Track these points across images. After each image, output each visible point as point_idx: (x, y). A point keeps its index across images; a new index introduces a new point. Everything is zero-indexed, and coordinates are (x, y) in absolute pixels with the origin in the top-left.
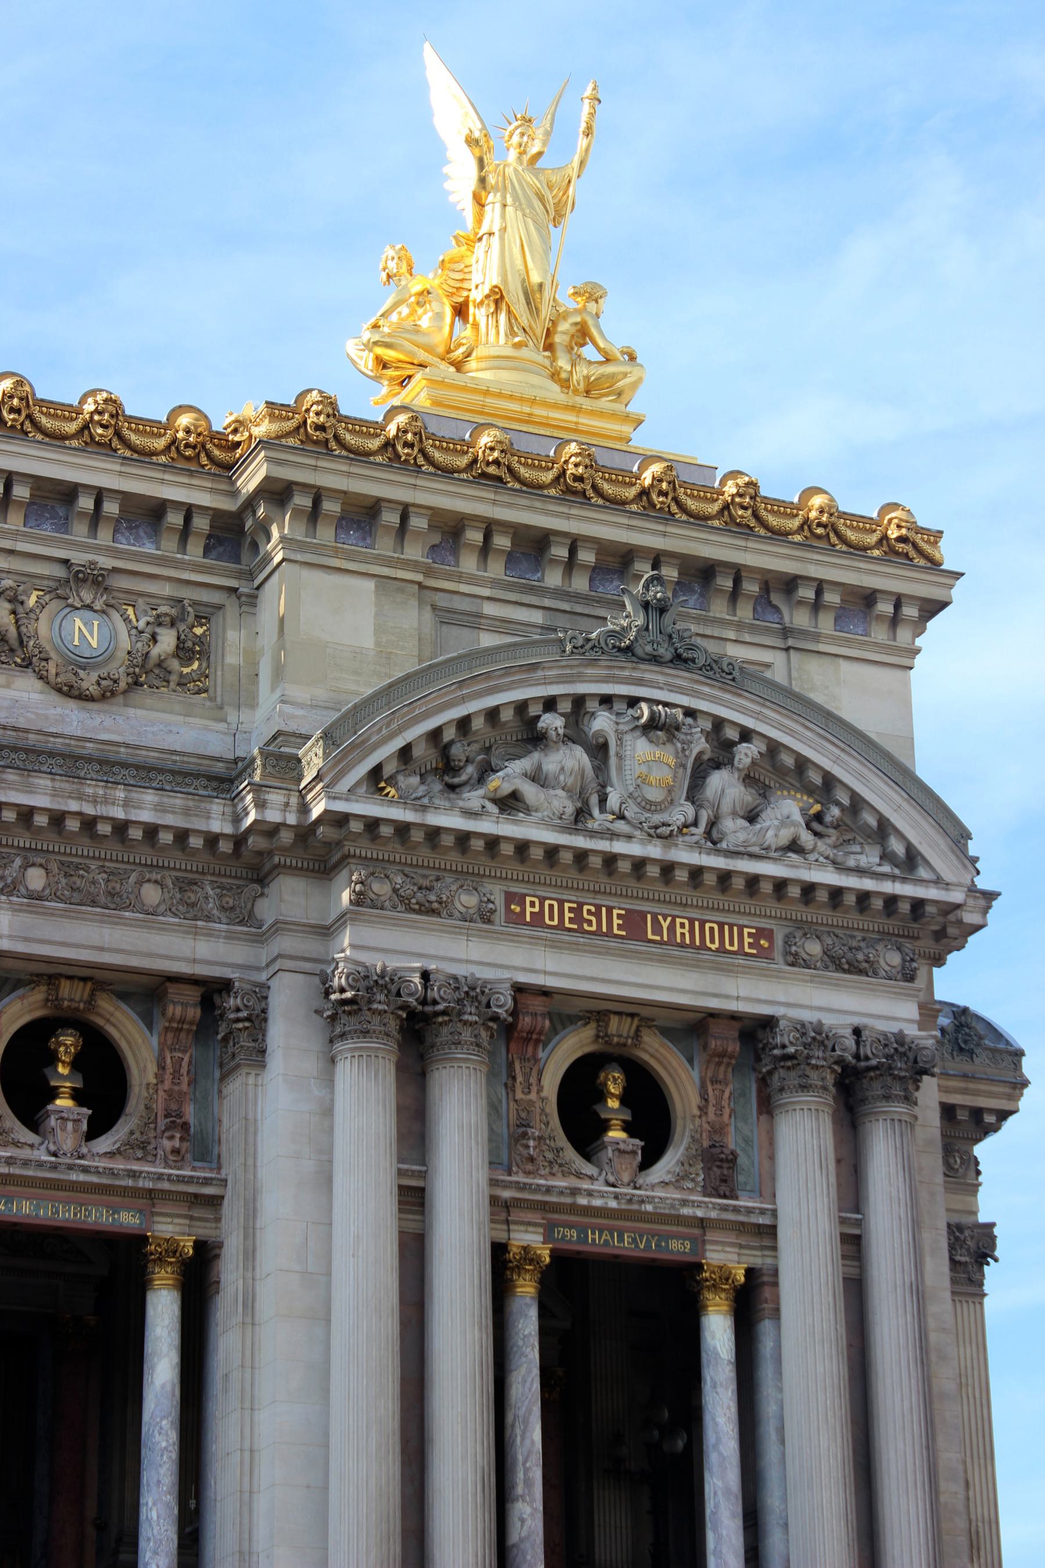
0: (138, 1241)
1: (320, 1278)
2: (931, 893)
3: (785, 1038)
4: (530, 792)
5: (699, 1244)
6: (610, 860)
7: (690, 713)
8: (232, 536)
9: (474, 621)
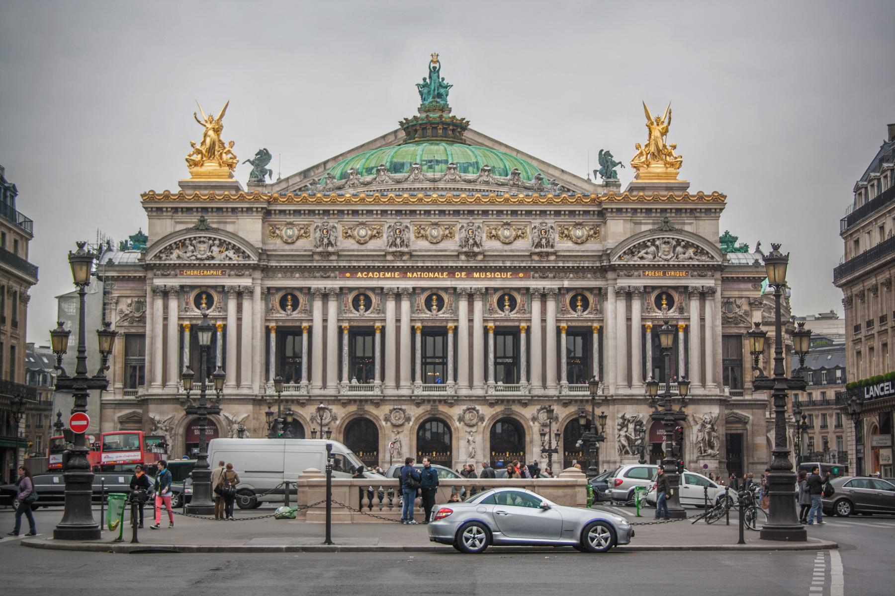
0: (591, 327)
1: (615, 333)
3: (690, 290)
4: (645, 256)
8: (602, 214)
9: (641, 223)
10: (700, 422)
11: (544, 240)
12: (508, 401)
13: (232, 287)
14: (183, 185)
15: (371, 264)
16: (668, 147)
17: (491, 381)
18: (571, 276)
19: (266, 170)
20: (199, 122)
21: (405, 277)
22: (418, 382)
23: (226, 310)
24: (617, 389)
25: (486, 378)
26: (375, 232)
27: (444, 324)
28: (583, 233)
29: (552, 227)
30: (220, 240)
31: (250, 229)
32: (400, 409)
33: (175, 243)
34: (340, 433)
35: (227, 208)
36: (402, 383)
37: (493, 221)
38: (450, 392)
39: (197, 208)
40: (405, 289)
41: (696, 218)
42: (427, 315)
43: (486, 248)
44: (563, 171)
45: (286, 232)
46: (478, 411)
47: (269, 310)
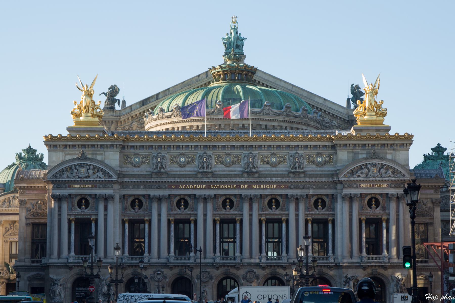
0: (327, 219)
1: (342, 223)
2: (405, 179)
3: (390, 196)
4: (360, 175)
5: (382, 216)
6: (370, 180)
7: (379, 163)
8: (334, 147)
9: (359, 153)
10: (395, 280)
11: (297, 165)
13: (101, 195)
14: (69, 129)
15: (187, 180)
16: (378, 103)
17: (264, 254)
18: (314, 187)
19: (116, 100)
20: (79, 89)
21: (209, 187)
22: (218, 254)
23: (97, 209)
24: (343, 258)
25: (261, 252)
26: (190, 160)
27: (234, 217)
28: (322, 159)
29: (302, 156)
30: (93, 165)
31: (113, 158)
32: (207, 272)
34: (169, 286)
35: (98, 145)
36: (208, 255)
37: (265, 152)
38: (238, 260)
39: (79, 145)
40: (210, 196)
41: (394, 150)
42: (223, 212)
43: (261, 169)
44: (325, 99)
45: (134, 160)
46: (255, 273)
47: (124, 209)
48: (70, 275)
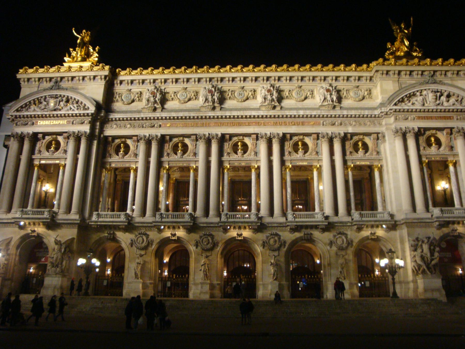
4: (416, 102)
12: (307, 227)
17: (290, 212)
33: (34, 100)
36: (212, 212)
48: (19, 237)
